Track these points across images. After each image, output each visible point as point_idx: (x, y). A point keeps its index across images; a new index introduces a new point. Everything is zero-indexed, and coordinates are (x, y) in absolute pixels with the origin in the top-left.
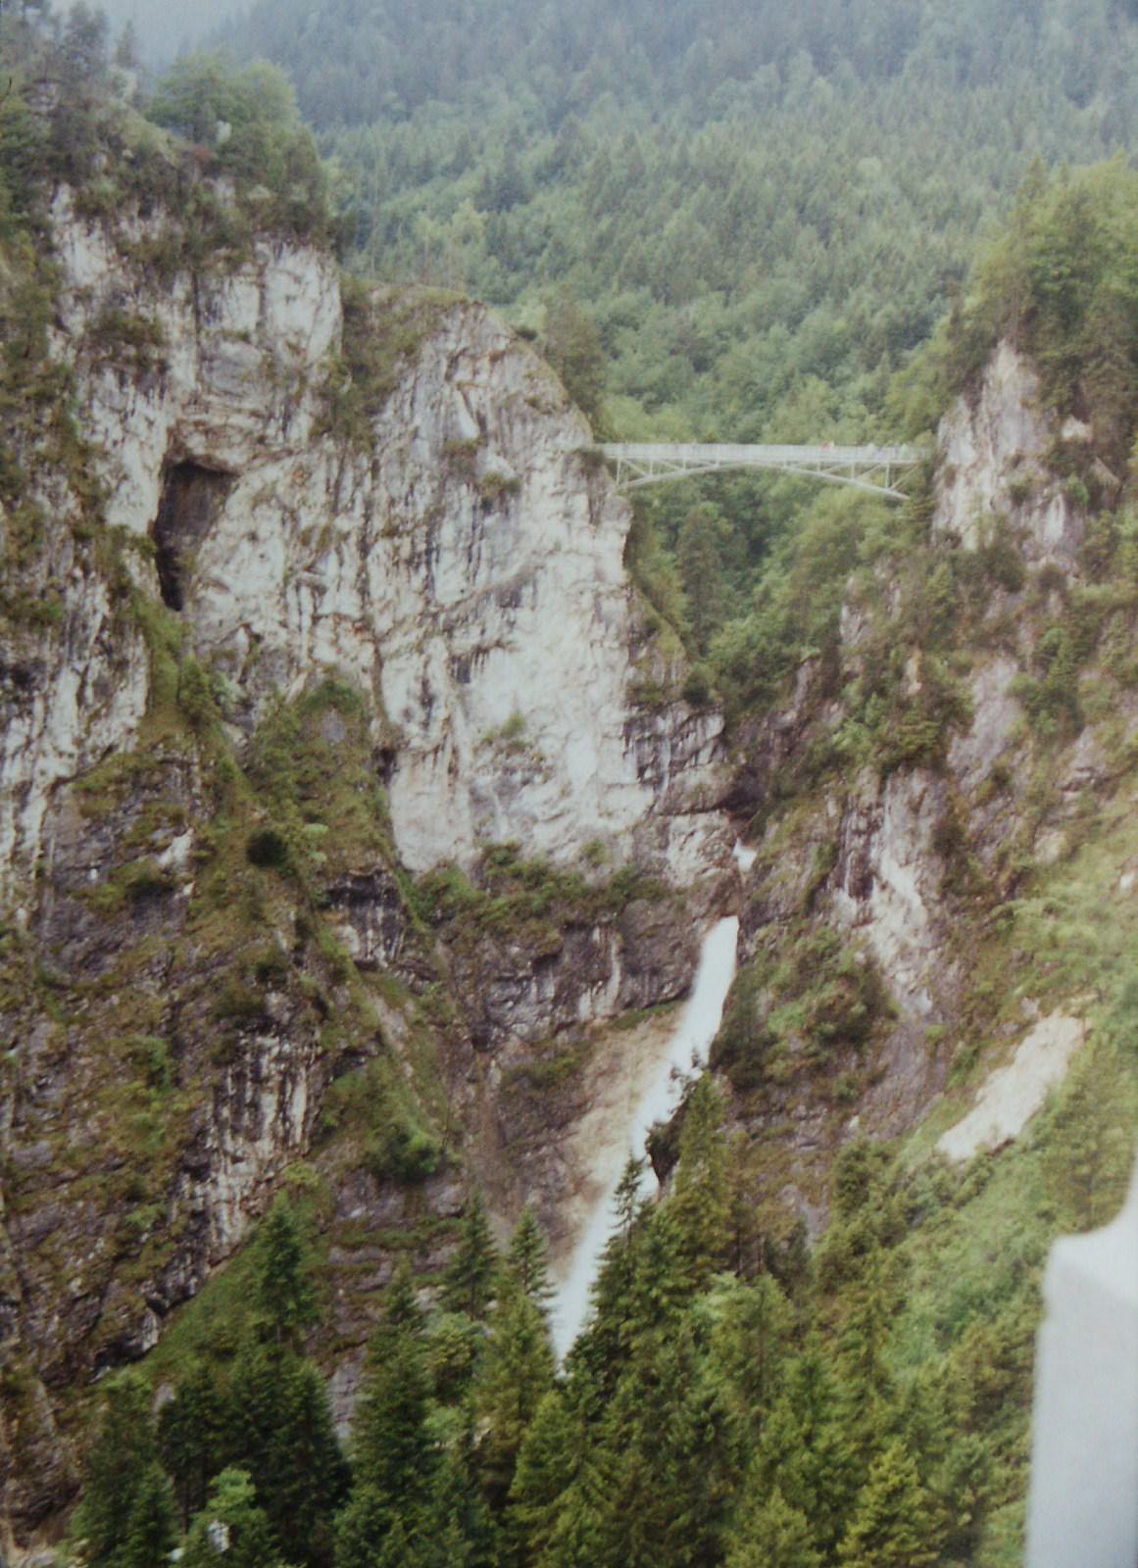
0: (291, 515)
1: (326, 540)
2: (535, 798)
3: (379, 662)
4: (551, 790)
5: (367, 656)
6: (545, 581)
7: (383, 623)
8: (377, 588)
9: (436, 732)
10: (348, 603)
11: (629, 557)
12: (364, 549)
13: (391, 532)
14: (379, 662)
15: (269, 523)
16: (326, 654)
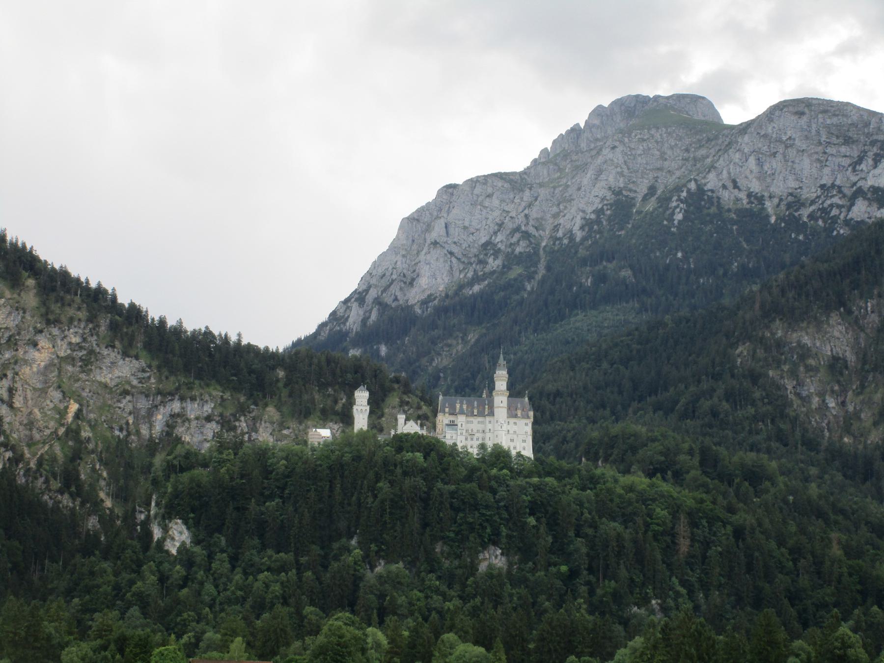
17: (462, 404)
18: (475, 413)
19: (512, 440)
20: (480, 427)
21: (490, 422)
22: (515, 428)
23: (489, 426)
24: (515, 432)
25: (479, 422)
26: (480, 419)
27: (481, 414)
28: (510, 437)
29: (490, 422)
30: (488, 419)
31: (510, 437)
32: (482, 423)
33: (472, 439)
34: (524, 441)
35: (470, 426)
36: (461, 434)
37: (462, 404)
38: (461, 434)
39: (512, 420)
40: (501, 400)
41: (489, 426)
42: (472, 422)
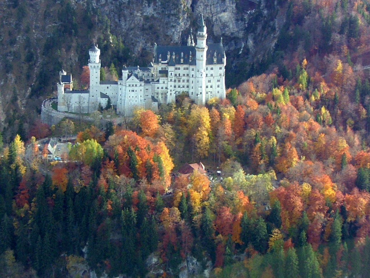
0: (204, 3)
1: (207, 6)
2: (226, 29)
3: (212, 16)
4: (228, 29)
5: (211, 16)
6: (228, 10)
7: (213, 13)
8: (212, 10)
9: (218, 23)
10: (209, 11)
11: (236, 7)
12: (211, 6)
13: (213, 5)
14: (212, 16)
15: (202, 4)
16: (207, 16)
17: (171, 55)
18: (182, 62)
19: (209, 81)
20: (186, 72)
21: (193, 70)
22: (212, 72)
23: (193, 73)
24: (212, 75)
25: (184, 69)
26: (186, 66)
27: (186, 62)
28: (208, 79)
29: (193, 70)
30: (191, 67)
31: (208, 79)
32: (187, 69)
33: (179, 81)
34: (219, 81)
35: (178, 72)
36: (171, 80)
37: (171, 55)
38: (171, 80)
39: (210, 67)
40: (202, 56)
41: (193, 73)
42: (179, 69)
